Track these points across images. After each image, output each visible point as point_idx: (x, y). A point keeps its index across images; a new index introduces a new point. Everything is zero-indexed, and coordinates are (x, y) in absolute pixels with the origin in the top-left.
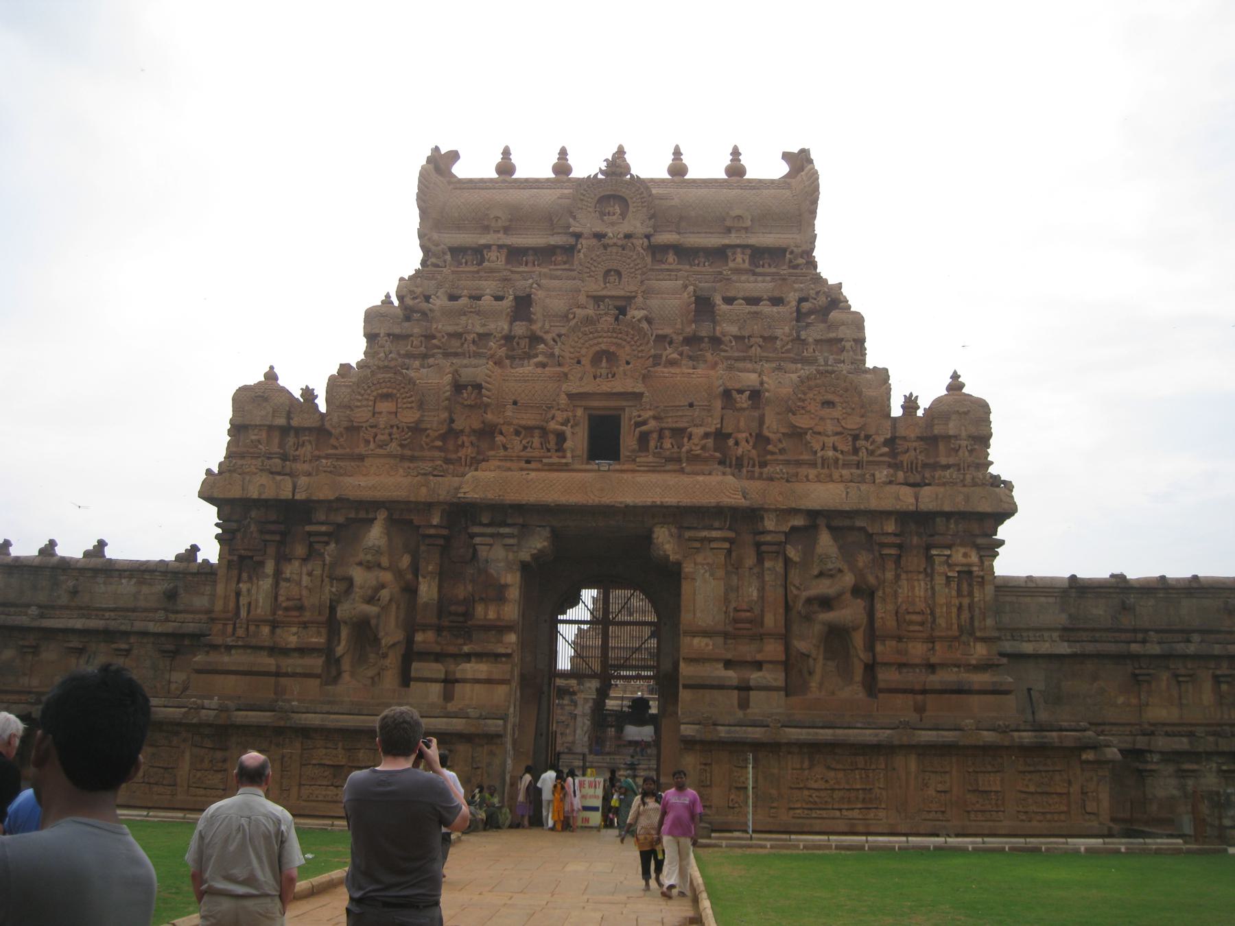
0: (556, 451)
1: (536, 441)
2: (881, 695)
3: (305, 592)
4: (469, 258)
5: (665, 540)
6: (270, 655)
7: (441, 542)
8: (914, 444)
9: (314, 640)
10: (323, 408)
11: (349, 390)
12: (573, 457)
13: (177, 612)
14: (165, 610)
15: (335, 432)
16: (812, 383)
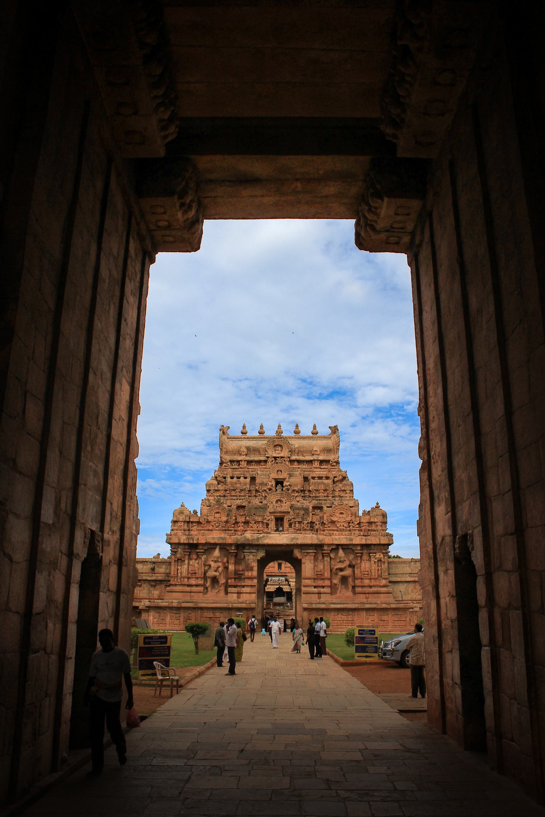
0: (266, 528)
1: (261, 525)
2: (356, 595)
3: (196, 569)
4: (235, 463)
5: (297, 553)
6: (188, 587)
7: (235, 554)
8: (366, 524)
9: (200, 582)
10: (199, 515)
11: (207, 510)
12: (271, 530)
13: (155, 573)
14: (152, 573)
15: (203, 523)
16: (337, 508)
